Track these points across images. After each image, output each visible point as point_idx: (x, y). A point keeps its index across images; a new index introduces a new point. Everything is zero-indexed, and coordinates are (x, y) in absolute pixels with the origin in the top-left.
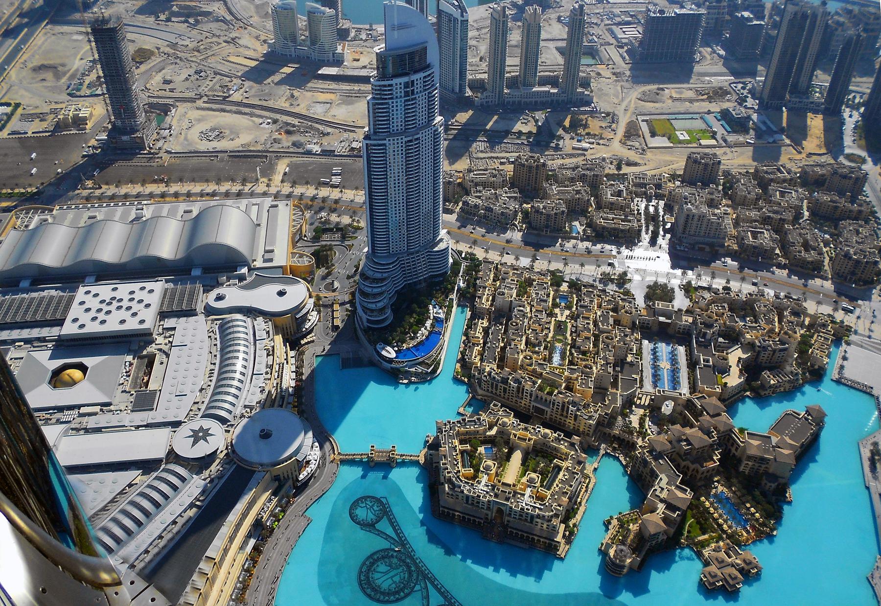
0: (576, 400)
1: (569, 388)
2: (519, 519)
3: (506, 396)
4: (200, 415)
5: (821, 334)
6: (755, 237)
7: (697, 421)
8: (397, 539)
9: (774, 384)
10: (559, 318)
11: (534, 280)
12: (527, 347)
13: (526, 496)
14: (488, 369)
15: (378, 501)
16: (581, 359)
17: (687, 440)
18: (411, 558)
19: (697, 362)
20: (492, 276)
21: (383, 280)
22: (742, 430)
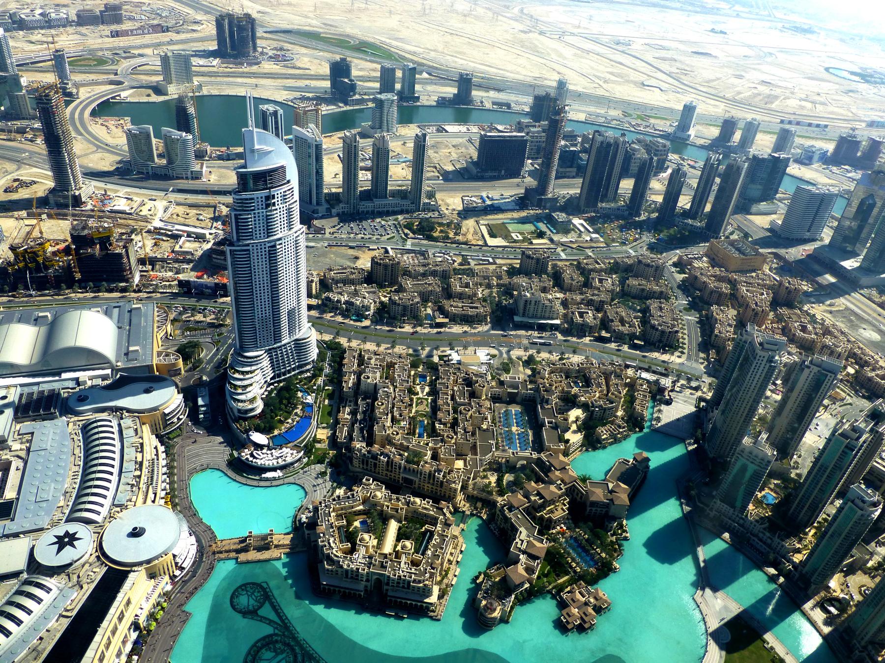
0: (440, 467)
1: (435, 457)
2: (397, 586)
3: (377, 470)
4: (64, 521)
5: (640, 392)
6: (581, 315)
7: (548, 476)
8: (279, 622)
9: (607, 438)
10: (421, 395)
11: (395, 364)
12: (393, 424)
13: (402, 565)
14: (358, 446)
15: (258, 586)
16: (443, 430)
17: (539, 494)
18: (295, 639)
19: (543, 425)
20: (356, 361)
21: (251, 372)
22: (584, 480)
